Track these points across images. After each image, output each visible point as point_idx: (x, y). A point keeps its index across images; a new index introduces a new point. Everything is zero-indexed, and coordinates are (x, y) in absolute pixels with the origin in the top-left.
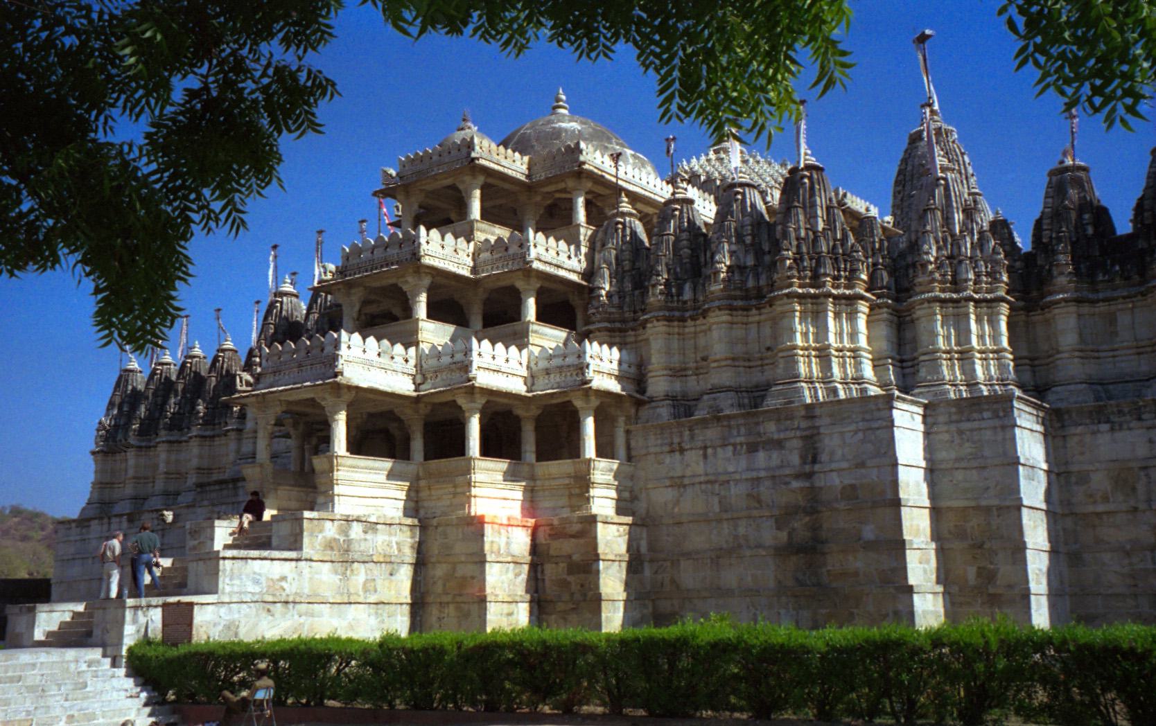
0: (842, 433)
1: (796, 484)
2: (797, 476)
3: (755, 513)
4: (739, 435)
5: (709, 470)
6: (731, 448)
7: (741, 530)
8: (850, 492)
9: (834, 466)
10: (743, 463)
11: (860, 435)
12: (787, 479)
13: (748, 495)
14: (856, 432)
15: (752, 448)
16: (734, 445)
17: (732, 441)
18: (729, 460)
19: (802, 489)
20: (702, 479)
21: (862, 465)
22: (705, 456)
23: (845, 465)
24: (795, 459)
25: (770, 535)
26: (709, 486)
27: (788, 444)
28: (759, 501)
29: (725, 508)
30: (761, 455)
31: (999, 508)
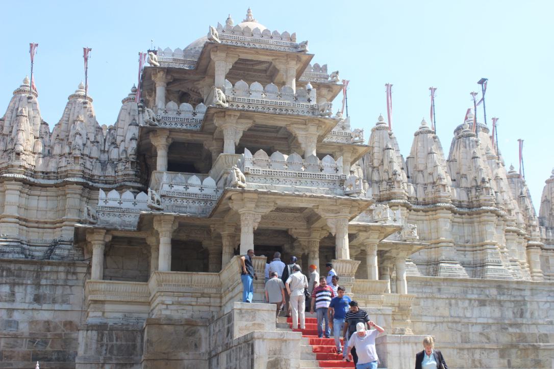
0: (538, 302)
1: (511, 330)
2: (511, 325)
4: (473, 294)
5: (453, 314)
6: (467, 302)
7: (477, 356)
10: (476, 312)
12: (506, 327)
13: (481, 334)
14: (546, 302)
15: (482, 303)
16: (470, 300)
17: (469, 296)
18: (466, 308)
19: (515, 333)
20: (450, 319)
22: (450, 305)
24: (509, 314)
26: (454, 325)
28: (488, 339)
29: (465, 340)
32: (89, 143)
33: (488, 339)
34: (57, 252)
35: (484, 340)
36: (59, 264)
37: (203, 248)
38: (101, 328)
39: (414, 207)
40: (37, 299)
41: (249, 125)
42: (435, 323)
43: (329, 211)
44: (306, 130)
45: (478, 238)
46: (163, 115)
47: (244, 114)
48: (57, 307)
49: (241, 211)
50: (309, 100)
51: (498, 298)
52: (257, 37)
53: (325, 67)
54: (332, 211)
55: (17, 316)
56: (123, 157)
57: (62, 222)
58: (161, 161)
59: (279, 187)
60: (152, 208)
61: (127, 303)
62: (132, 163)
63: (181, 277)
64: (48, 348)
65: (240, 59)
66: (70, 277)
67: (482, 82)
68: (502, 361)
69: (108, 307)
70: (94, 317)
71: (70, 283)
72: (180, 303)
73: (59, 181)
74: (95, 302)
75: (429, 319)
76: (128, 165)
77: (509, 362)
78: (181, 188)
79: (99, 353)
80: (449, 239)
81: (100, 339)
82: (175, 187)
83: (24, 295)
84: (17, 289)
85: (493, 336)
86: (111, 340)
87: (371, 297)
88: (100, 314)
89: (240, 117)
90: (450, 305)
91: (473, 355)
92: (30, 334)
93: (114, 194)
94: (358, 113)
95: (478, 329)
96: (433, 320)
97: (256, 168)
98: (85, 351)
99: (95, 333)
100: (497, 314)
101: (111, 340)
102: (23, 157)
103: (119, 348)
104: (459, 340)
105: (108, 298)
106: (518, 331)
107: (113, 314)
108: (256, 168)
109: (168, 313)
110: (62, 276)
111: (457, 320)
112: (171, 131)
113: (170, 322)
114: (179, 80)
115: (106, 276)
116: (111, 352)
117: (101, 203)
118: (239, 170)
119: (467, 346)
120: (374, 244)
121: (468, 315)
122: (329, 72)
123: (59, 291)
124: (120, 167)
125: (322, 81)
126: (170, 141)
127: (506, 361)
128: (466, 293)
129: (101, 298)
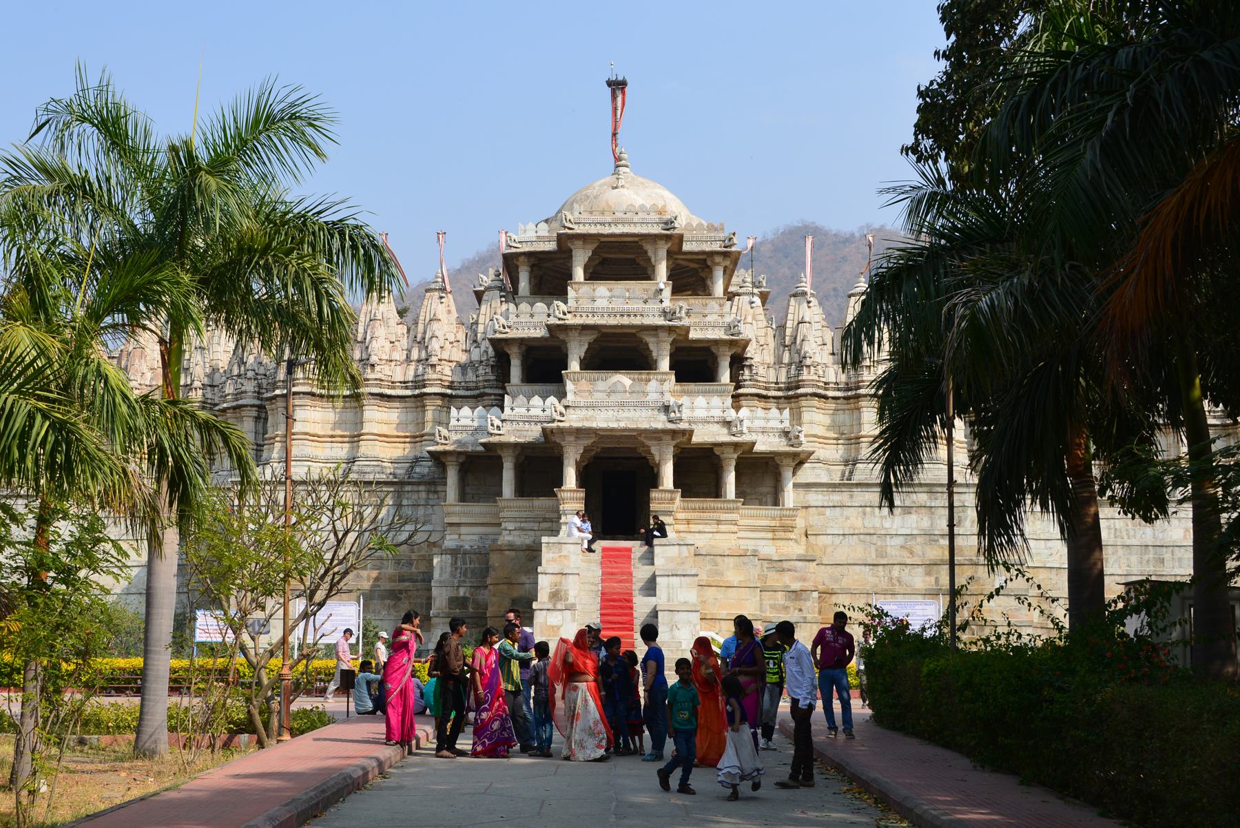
5: (866, 524)
22: (864, 514)
28: (911, 553)
32: (448, 345)
33: (911, 553)
34: (418, 470)
35: (905, 553)
36: (419, 484)
38: (454, 552)
39: (830, 394)
41: (594, 337)
44: (656, 336)
46: (515, 319)
47: (585, 328)
50: (661, 301)
52: (619, 215)
54: (656, 439)
56: (484, 358)
57: (422, 436)
58: (516, 372)
63: (524, 502)
64: (414, 570)
66: (431, 496)
68: (928, 578)
69: (463, 530)
70: (451, 541)
71: (431, 502)
72: (522, 529)
73: (417, 392)
74: (451, 524)
76: (489, 370)
78: (523, 411)
79: (454, 576)
82: (517, 410)
85: (918, 550)
86: (465, 563)
87: (724, 516)
90: (864, 514)
93: (466, 411)
95: (899, 541)
97: (579, 399)
98: (441, 575)
100: (926, 524)
101: (465, 563)
102: (377, 368)
103: (473, 570)
104: (874, 556)
107: (469, 538)
108: (579, 399)
109: (510, 538)
110: (423, 495)
111: (872, 531)
113: (512, 547)
115: (463, 497)
116: (465, 576)
117: (453, 422)
121: (887, 524)
123: (421, 511)
124: (481, 371)
126: (524, 348)
127: (933, 579)
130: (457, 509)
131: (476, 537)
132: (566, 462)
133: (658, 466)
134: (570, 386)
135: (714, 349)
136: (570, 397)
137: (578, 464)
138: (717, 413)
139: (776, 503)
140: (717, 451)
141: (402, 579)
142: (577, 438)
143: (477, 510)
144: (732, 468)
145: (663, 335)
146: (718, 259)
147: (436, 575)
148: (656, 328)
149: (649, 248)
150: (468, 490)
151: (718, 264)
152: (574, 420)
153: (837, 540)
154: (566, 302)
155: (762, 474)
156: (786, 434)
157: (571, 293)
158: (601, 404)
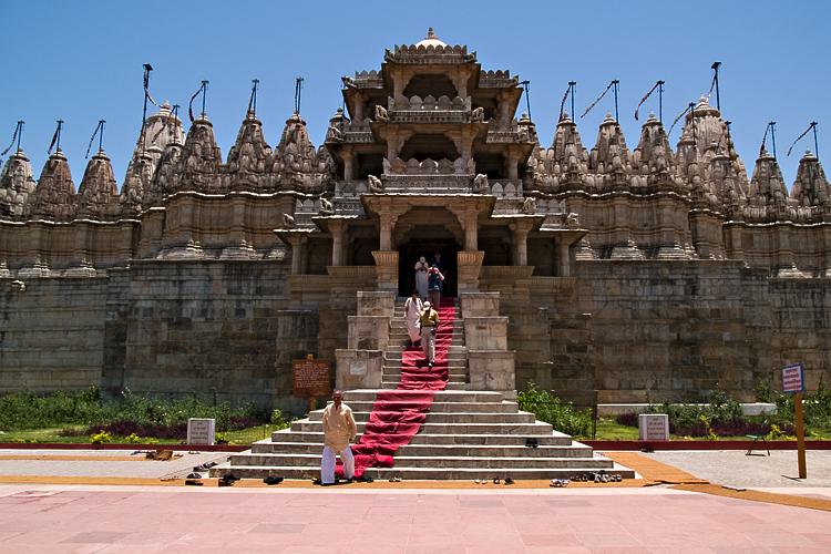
1: (682, 306)
2: (682, 302)
3: (656, 321)
5: (624, 292)
8: (716, 313)
9: (707, 297)
11: (722, 282)
13: (652, 310)
15: (654, 282)
16: (642, 280)
17: (639, 276)
21: (724, 298)
22: (621, 284)
23: (713, 298)
24: (682, 291)
25: (665, 334)
27: (677, 283)
28: (658, 315)
29: (635, 316)
30: (659, 287)
31: (761, 328)
33: (658, 315)
37: (511, 240)
38: (295, 315)
40: (259, 291)
42: (607, 302)
43: (458, 208)
44: (461, 135)
45: (656, 222)
47: (402, 126)
48: (275, 297)
49: (380, 213)
51: (670, 277)
52: (430, 53)
53: (507, 72)
54: (462, 208)
55: (243, 305)
58: (347, 172)
59: (414, 191)
60: (324, 214)
61: (320, 292)
62: (333, 174)
63: (350, 270)
65: (417, 76)
67: (716, 66)
69: (304, 296)
70: (294, 306)
74: (294, 292)
75: (600, 299)
77: (678, 335)
80: (624, 224)
81: (294, 325)
83: (248, 288)
84: (243, 284)
87: (518, 282)
88: (298, 302)
89: (400, 128)
91: (643, 328)
92: (255, 319)
94: (539, 113)
95: (648, 306)
96: (604, 299)
98: (284, 333)
99: (290, 318)
104: (630, 317)
105: (304, 289)
106: (689, 307)
107: (309, 303)
112: (353, 145)
114: (364, 97)
118: (375, 178)
119: (638, 321)
120: (523, 234)
121: (639, 293)
122: (511, 78)
125: (505, 85)
126: (355, 153)
127: (675, 335)
128: (638, 273)
129: (298, 289)
130: (299, 280)
131: (316, 303)
132: (383, 228)
133: (463, 234)
134: (386, 163)
135: (505, 154)
136: (387, 173)
137: (394, 233)
138: (511, 197)
139: (554, 271)
140: (512, 227)
141: (260, 338)
142: (392, 208)
143: (315, 279)
144: (525, 242)
145: (466, 133)
146: (505, 95)
147: (280, 334)
148: (460, 127)
149: (453, 78)
150: (313, 267)
151: (506, 100)
152: (391, 191)
153: (600, 306)
154: (386, 107)
155: (547, 251)
156: (563, 219)
157: (391, 102)
158: (411, 187)
